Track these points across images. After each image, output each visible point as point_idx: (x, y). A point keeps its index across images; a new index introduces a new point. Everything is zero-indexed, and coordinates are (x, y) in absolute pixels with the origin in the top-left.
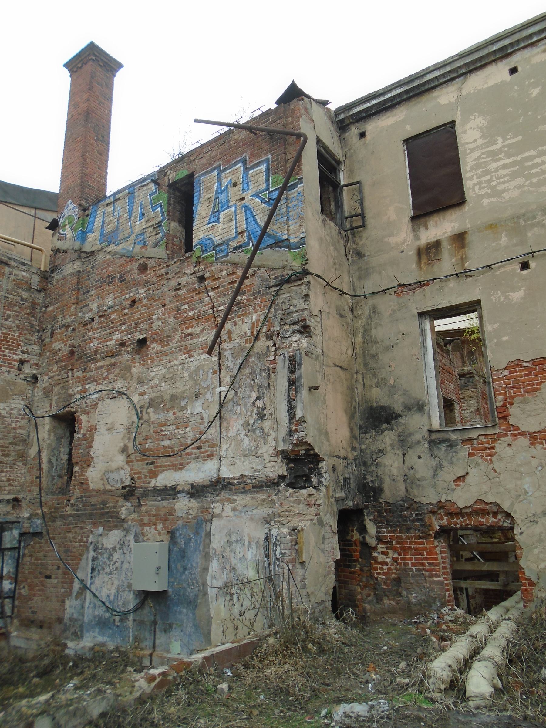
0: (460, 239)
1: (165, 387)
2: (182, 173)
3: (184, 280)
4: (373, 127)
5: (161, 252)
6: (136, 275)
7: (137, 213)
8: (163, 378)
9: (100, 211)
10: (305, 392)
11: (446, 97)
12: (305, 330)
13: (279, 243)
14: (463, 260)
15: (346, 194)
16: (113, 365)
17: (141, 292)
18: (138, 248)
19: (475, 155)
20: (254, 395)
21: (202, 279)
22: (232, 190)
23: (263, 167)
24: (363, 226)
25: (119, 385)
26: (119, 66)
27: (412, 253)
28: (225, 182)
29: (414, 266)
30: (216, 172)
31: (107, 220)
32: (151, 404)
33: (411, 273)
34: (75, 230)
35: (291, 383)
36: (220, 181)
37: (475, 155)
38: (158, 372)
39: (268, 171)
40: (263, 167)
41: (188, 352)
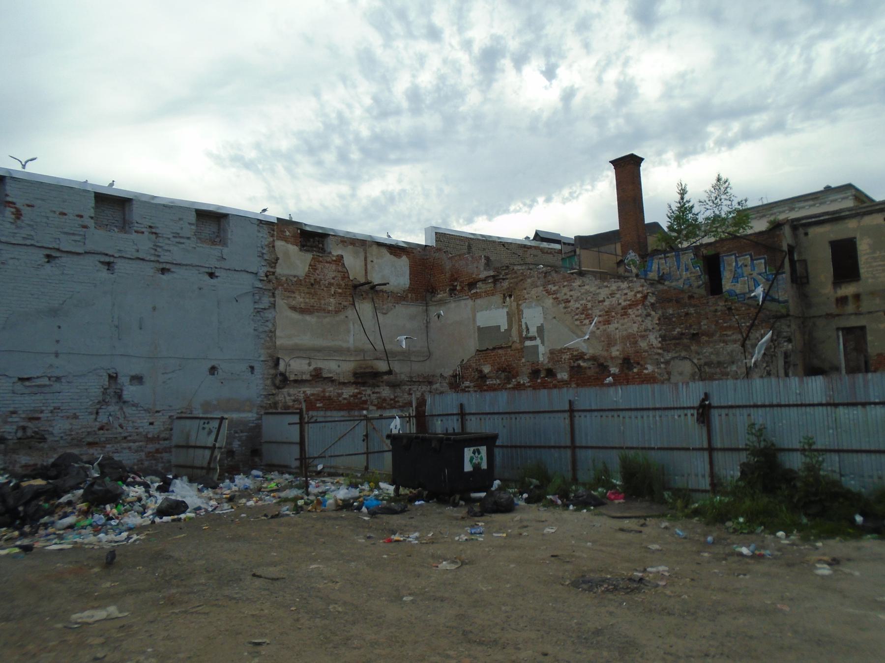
0: (857, 297)
1: (713, 357)
2: (710, 252)
3: (719, 308)
4: (812, 231)
5: (702, 291)
6: (687, 300)
7: (683, 267)
8: (712, 353)
9: (656, 261)
10: (792, 367)
11: (852, 224)
12: (789, 341)
13: (773, 300)
14: (858, 307)
15: (797, 265)
16: (678, 344)
17: (692, 310)
18: (686, 287)
19: (866, 257)
20: (765, 365)
21: (730, 309)
22: (744, 269)
23: (763, 261)
24: (808, 282)
25: (683, 354)
26: (642, 159)
27: (833, 300)
28: (740, 264)
29: (834, 306)
30: (733, 257)
31: (661, 267)
32: (706, 364)
33: (833, 309)
34: (638, 269)
35: (785, 363)
36: (736, 262)
37: (866, 257)
38: (707, 350)
39: (765, 263)
40: (763, 261)
41: (726, 342)
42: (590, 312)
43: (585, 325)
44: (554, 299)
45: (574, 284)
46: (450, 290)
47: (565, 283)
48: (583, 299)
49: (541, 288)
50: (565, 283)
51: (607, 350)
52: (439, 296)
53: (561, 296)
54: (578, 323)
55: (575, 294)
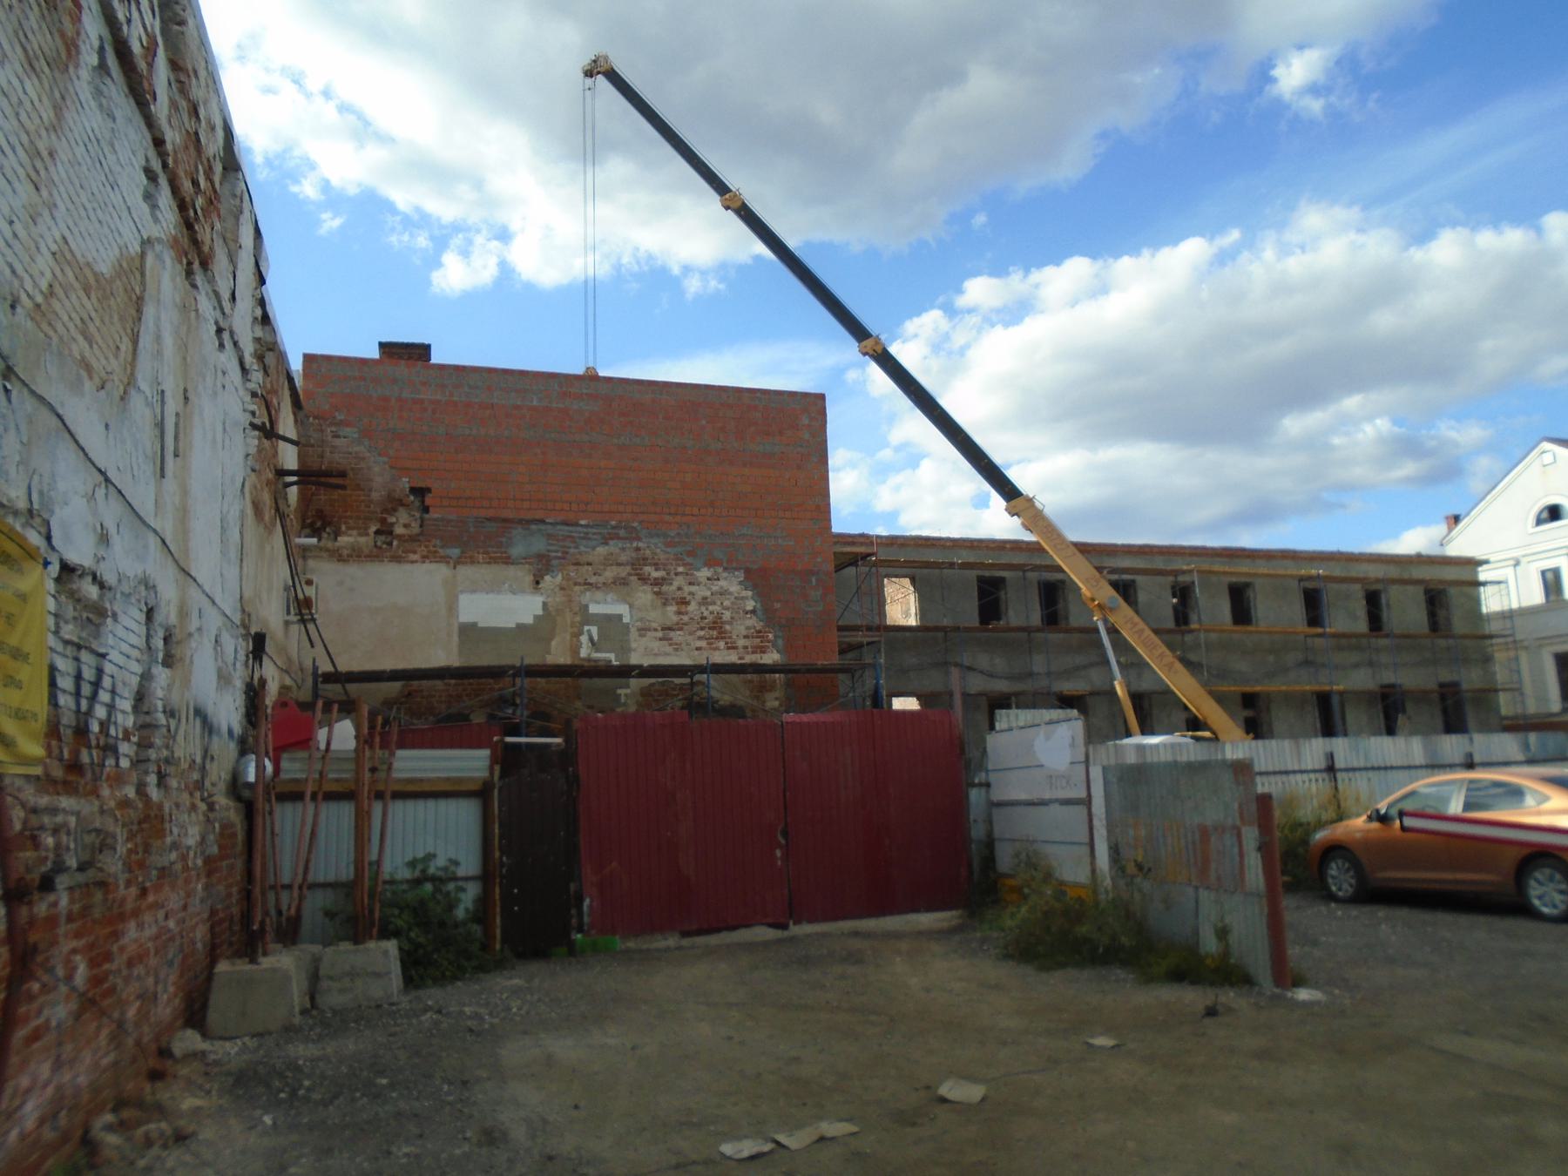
42: (728, 627)
43: (717, 649)
44: (657, 594)
45: (698, 574)
46: (377, 532)
47: (680, 569)
48: (714, 603)
49: (628, 569)
50: (680, 569)
51: (757, 698)
52: (344, 540)
53: (669, 589)
54: (703, 644)
55: (701, 592)
